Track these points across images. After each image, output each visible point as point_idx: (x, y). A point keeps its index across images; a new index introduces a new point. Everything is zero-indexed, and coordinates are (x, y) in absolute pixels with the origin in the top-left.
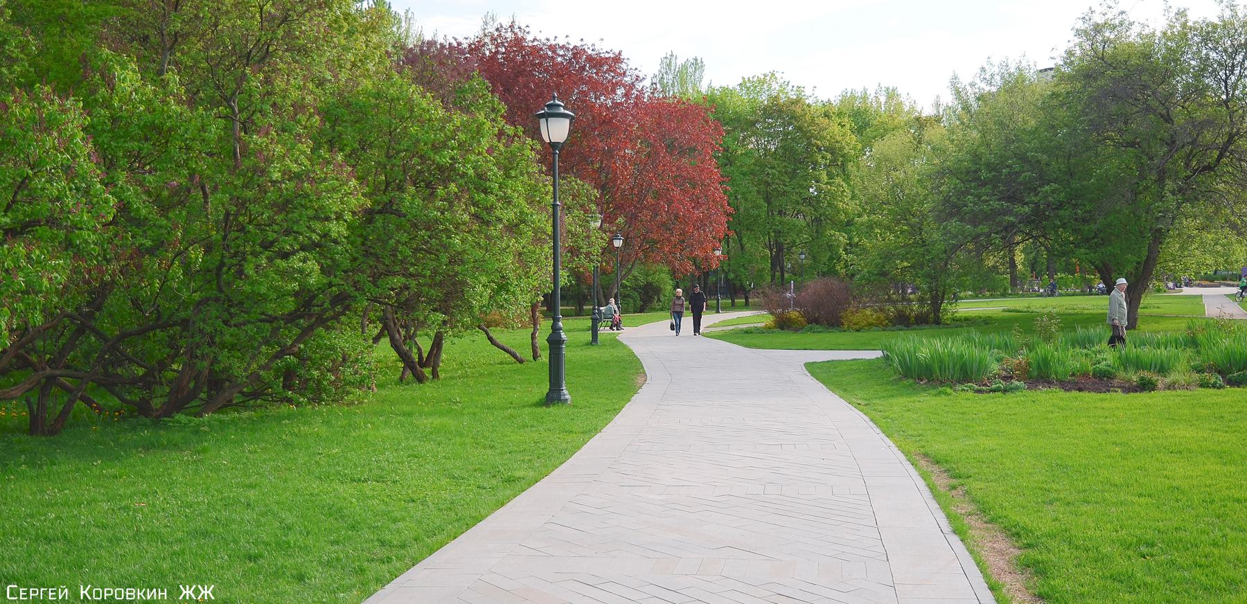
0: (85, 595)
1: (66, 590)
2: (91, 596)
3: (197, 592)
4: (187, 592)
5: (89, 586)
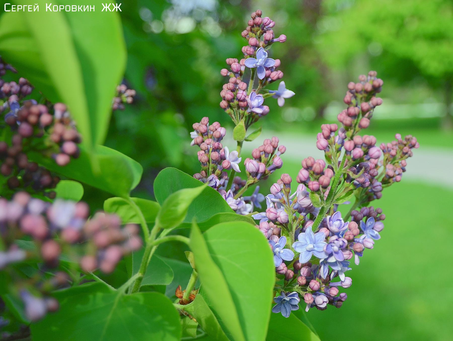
0: (48, 9)
1: (38, 6)
2: (52, 9)
4: (106, 7)
5: (51, 4)
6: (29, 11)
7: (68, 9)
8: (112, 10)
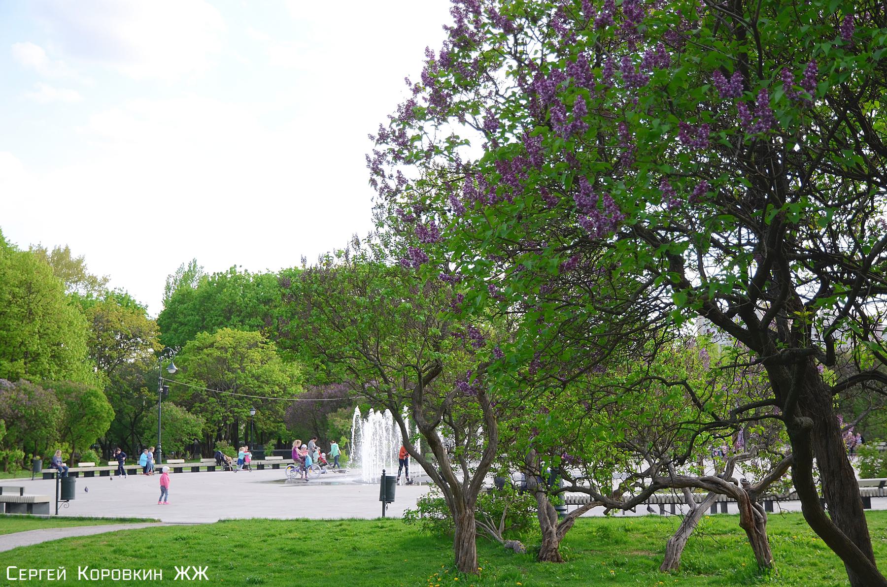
0: (82, 575)
1: (64, 571)
2: (89, 577)
3: (191, 572)
4: (182, 573)
6: (49, 579)
7: (116, 577)
8: (191, 578)
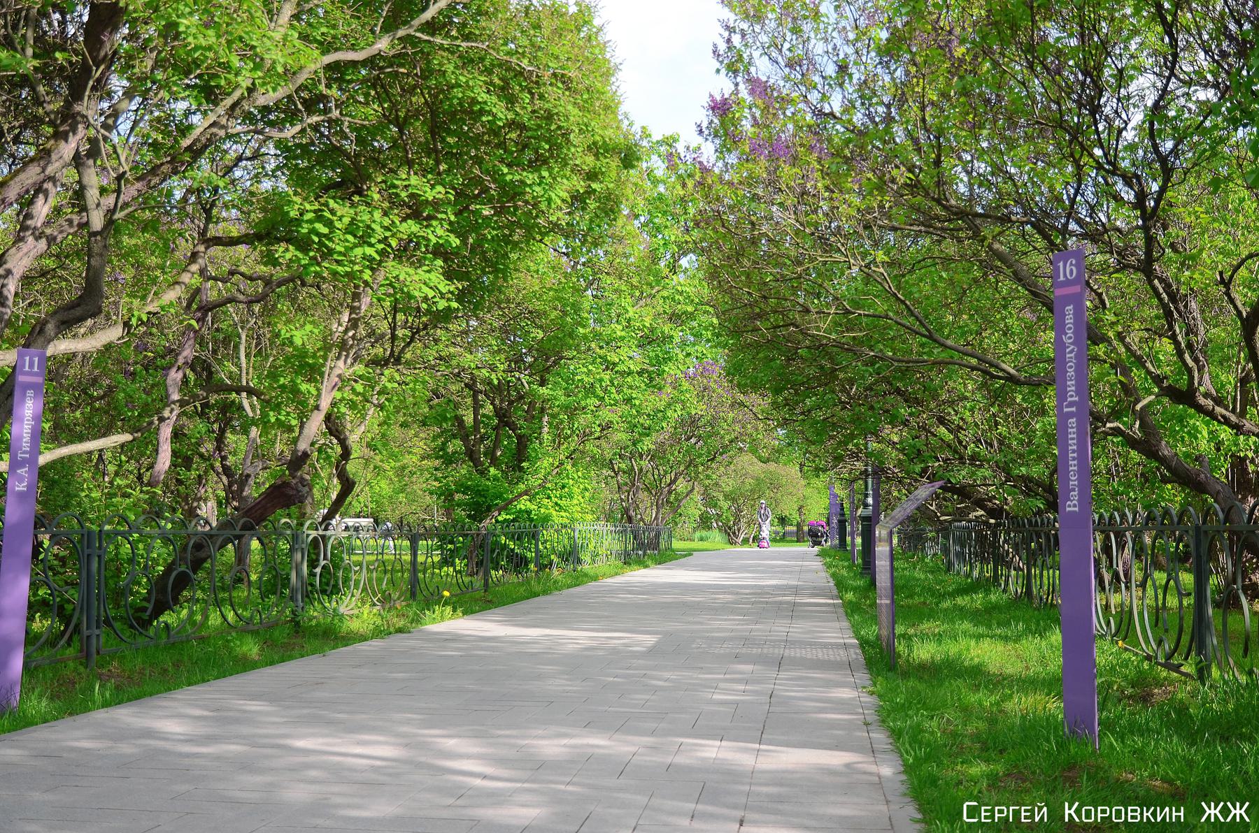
0: (1070, 815)
1: (1045, 809)
2: (1080, 817)
3: (1225, 812)
5: (1077, 804)
6: (1023, 820)
8: (1225, 819)
